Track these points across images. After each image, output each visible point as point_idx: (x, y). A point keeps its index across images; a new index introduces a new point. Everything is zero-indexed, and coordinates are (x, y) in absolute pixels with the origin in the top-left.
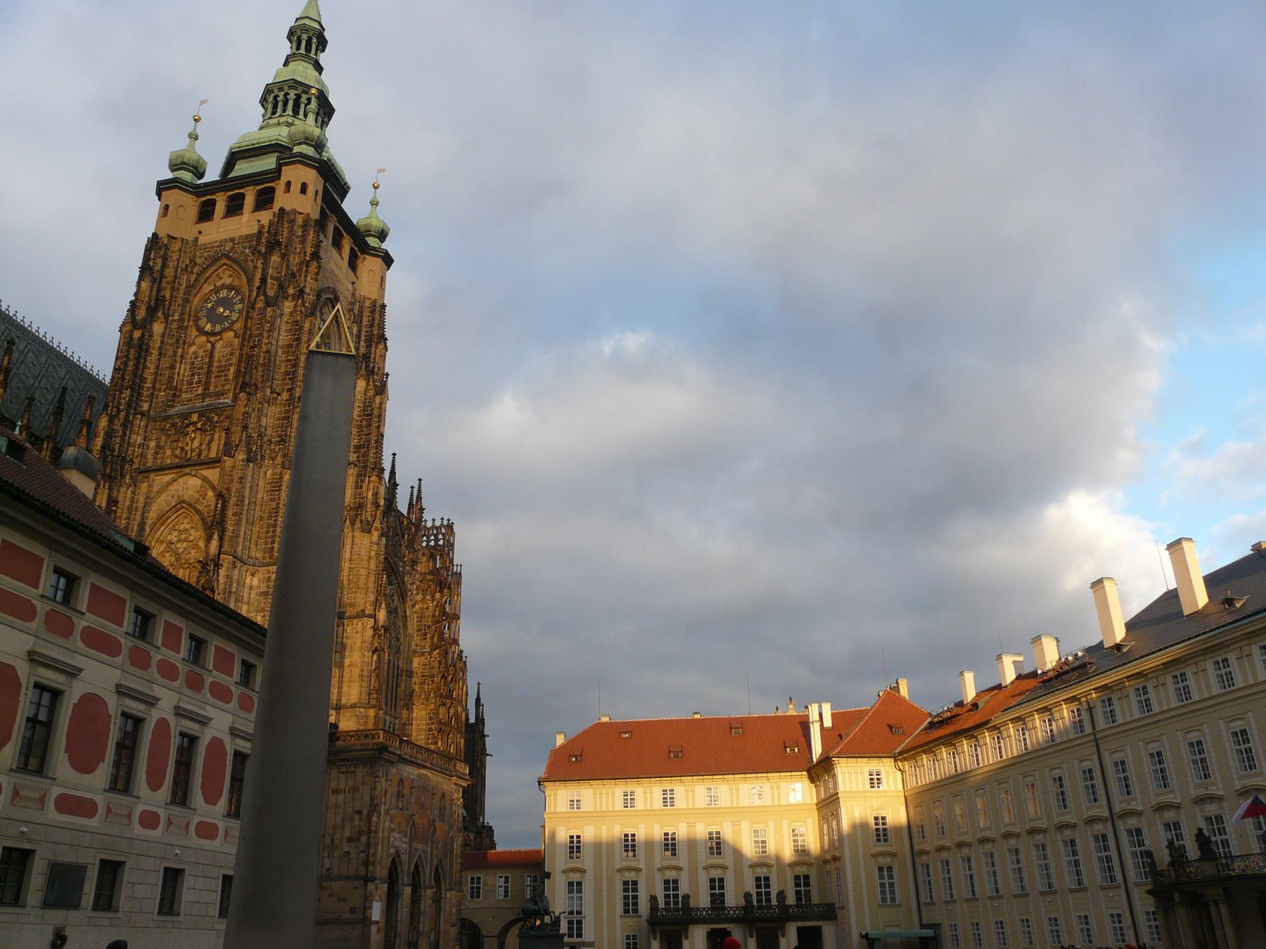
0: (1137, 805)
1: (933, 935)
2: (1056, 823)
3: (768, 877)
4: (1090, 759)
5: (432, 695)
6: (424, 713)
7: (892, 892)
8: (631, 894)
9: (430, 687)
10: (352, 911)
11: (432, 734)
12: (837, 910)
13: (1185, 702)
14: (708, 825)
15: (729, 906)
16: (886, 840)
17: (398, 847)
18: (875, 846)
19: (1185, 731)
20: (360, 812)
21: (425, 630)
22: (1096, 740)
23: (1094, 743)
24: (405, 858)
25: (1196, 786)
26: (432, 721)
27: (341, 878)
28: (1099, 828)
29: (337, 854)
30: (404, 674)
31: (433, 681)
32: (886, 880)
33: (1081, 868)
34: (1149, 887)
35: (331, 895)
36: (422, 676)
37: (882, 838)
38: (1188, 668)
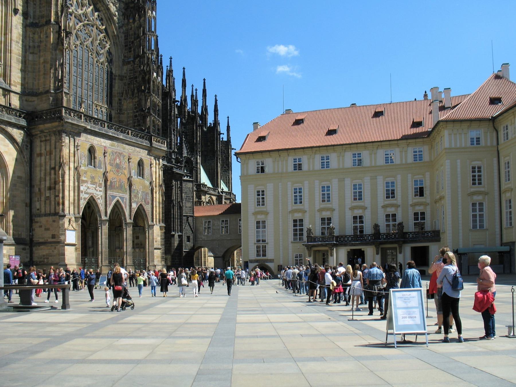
1: (509, 250)
3: (395, 214)
5: (136, 91)
6: (131, 104)
8: (298, 228)
9: (135, 85)
10: (53, 236)
11: (138, 119)
12: (441, 234)
14: (353, 180)
15: (366, 234)
16: (480, 184)
17: (93, 194)
18: (471, 187)
20: (54, 168)
21: (130, 45)
24: (100, 202)
26: (137, 110)
27: (46, 215)
29: (43, 199)
30: (117, 78)
31: (136, 81)
35: (41, 227)
36: (130, 79)
37: (477, 182)
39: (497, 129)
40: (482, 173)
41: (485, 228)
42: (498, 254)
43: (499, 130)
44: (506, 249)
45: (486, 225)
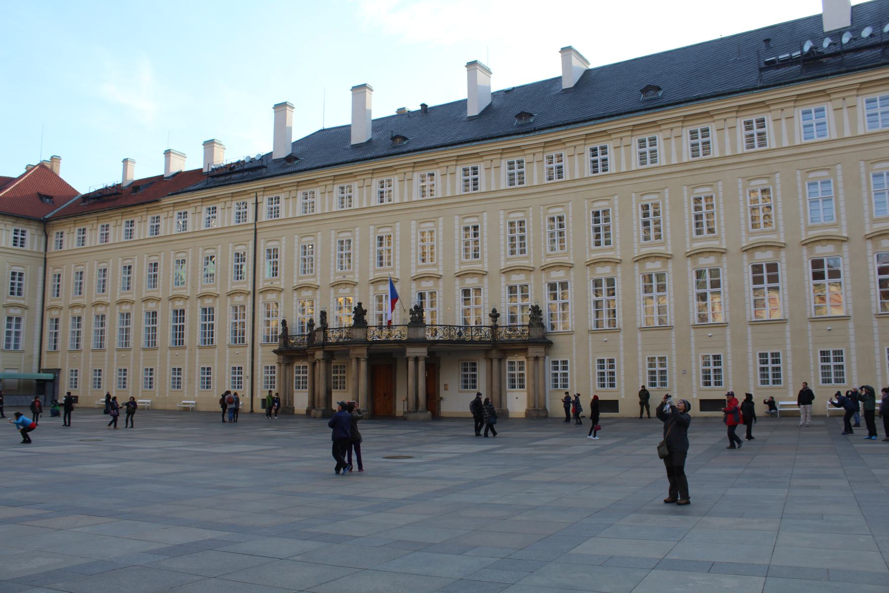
0: (281, 283)
2: (199, 293)
4: (185, 252)
7: (17, 340)
13: (273, 218)
16: (19, 294)
18: (8, 297)
19: (338, 231)
22: (256, 230)
23: (254, 232)
25: (337, 274)
28: (239, 299)
32: (13, 330)
33: (130, 334)
34: (277, 348)
38: (318, 188)
39: (47, 233)
40: (23, 282)
41: (20, 349)
42: (36, 382)
43: (50, 234)
44: (50, 376)
45: (22, 345)
